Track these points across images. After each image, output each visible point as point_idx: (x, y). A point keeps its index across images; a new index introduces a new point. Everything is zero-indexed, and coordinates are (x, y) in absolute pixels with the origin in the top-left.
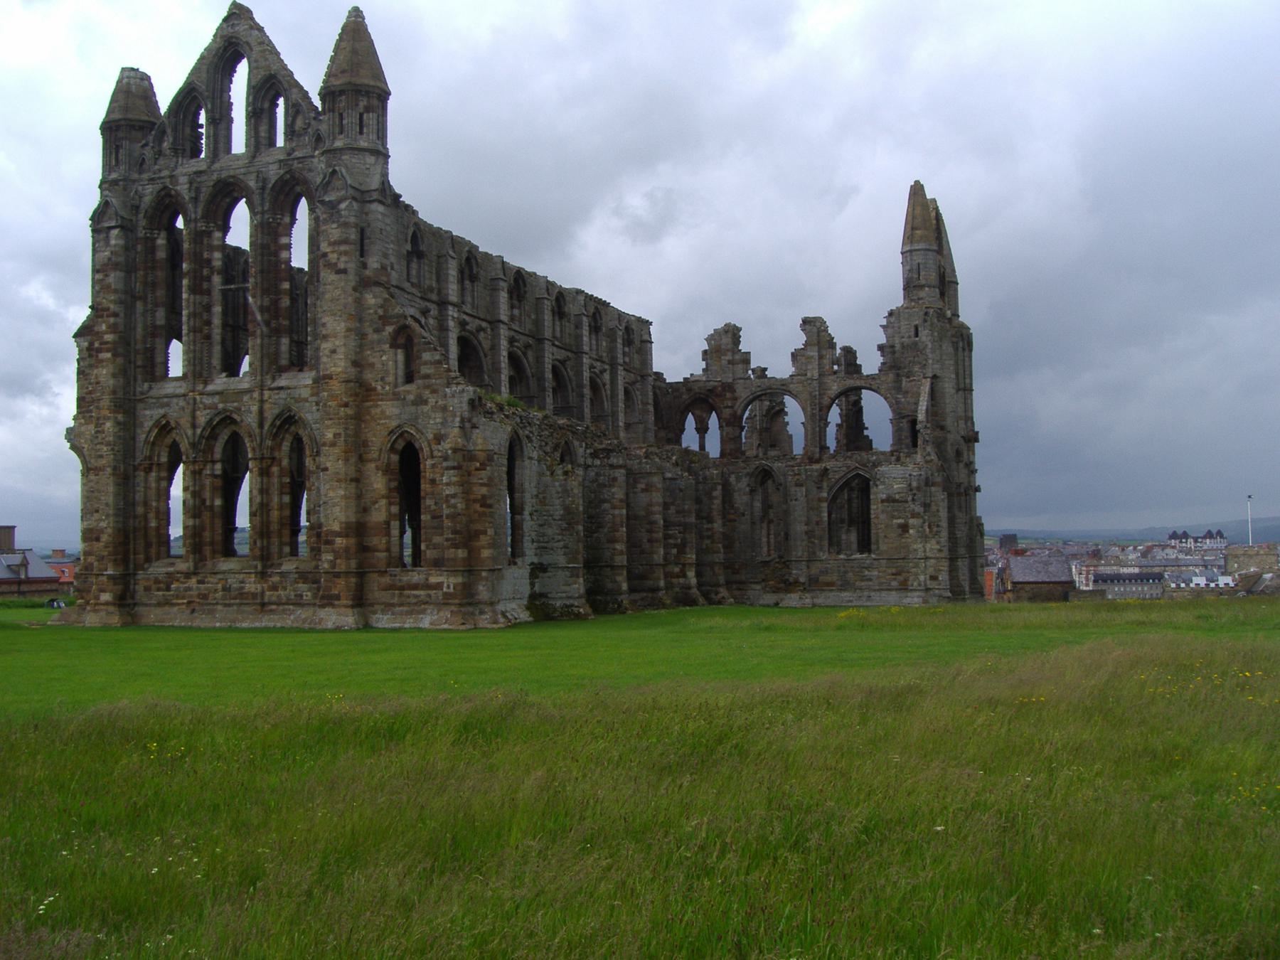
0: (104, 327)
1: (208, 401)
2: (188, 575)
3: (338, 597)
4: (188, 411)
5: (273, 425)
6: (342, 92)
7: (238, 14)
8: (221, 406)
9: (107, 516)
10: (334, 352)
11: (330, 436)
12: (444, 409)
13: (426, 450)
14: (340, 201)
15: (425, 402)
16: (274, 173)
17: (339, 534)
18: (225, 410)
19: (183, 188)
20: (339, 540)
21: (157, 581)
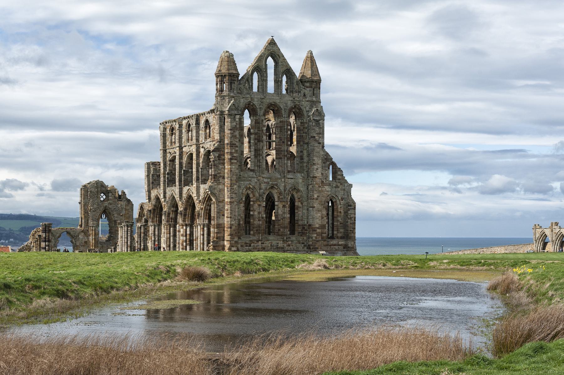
0: (233, 151)
1: (266, 180)
2: (258, 241)
3: (318, 248)
4: (258, 184)
5: (289, 190)
6: (316, 82)
7: (272, 43)
8: (270, 183)
9: (235, 220)
10: (317, 169)
11: (316, 196)
12: (344, 190)
13: (338, 202)
14: (319, 120)
15: (339, 187)
16: (290, 105)
17: (318, 228)
18: (272, 184)
19: (256, 102)
20: (318, 230)
21: (246, 243)
